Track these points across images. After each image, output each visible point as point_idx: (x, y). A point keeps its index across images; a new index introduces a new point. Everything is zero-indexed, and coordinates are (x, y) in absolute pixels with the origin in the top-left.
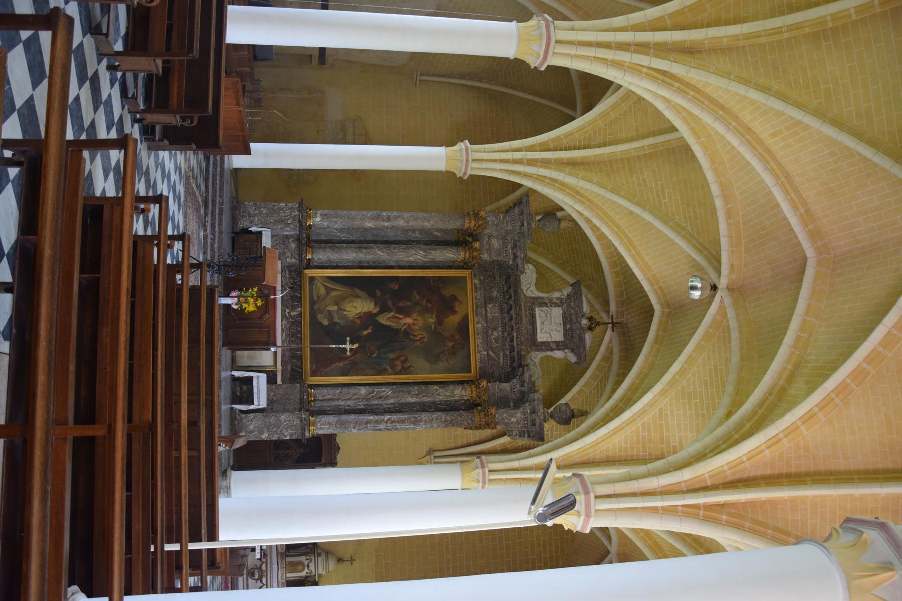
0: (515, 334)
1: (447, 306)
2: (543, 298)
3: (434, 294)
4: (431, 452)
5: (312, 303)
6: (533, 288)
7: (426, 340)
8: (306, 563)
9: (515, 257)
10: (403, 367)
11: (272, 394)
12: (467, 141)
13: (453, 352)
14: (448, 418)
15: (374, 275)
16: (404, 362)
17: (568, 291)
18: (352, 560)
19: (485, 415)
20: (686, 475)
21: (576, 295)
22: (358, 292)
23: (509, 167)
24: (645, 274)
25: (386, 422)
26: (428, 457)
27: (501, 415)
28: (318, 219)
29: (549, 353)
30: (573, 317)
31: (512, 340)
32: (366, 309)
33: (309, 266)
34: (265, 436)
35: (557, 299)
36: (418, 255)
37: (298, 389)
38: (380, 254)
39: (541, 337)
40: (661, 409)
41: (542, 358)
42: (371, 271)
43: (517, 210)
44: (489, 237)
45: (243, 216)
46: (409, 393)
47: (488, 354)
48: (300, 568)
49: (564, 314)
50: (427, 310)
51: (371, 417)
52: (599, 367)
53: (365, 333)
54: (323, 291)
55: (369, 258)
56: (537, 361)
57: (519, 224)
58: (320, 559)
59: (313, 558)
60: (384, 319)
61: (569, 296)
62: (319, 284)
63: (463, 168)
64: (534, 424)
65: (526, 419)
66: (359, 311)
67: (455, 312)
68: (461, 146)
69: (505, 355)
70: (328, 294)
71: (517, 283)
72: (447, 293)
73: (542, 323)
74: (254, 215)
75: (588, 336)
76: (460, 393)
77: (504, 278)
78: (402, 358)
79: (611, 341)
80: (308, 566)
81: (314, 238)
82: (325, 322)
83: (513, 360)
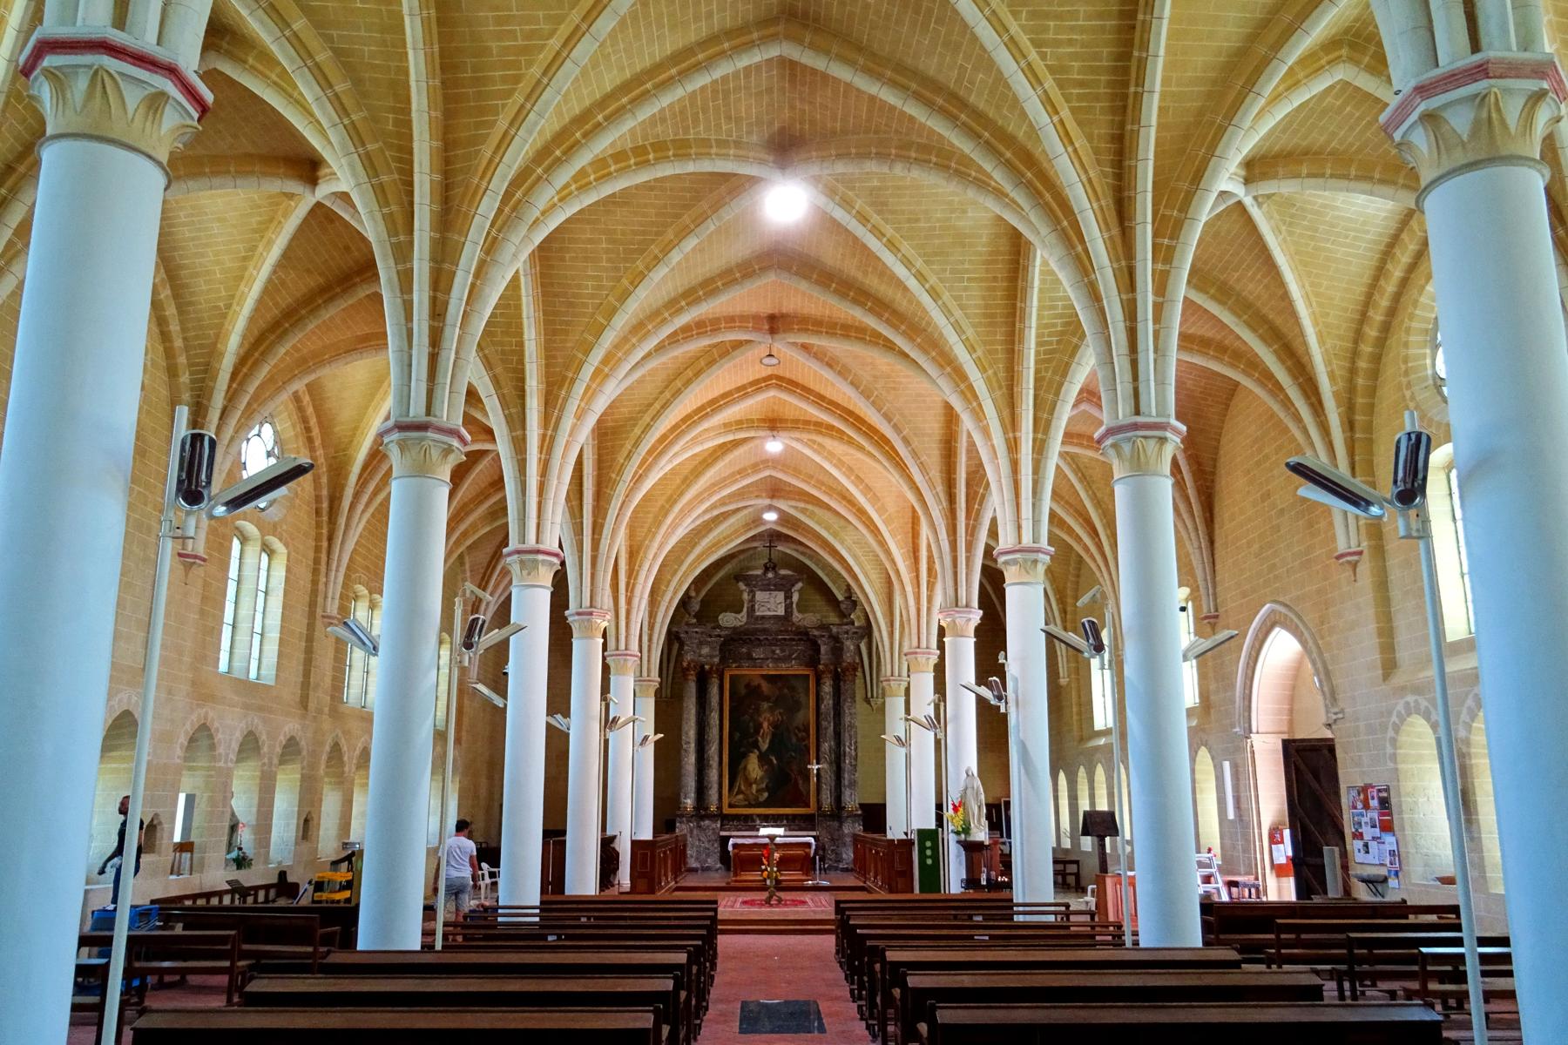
1: (754, 692)
3: (744, 702)
4: (867, 701)
5: (750, 806)
13: (793, 689)
17: (742, 586)
21: (748, 580)
27: (848, 657)
36: (715, 716)
38: (713, 750)
39: (781, 612)
50: (758, 711)
60: (765, 746)
72: (743, 691)
75: (783, 572)
76: (827, 688)
77: (734, 644)
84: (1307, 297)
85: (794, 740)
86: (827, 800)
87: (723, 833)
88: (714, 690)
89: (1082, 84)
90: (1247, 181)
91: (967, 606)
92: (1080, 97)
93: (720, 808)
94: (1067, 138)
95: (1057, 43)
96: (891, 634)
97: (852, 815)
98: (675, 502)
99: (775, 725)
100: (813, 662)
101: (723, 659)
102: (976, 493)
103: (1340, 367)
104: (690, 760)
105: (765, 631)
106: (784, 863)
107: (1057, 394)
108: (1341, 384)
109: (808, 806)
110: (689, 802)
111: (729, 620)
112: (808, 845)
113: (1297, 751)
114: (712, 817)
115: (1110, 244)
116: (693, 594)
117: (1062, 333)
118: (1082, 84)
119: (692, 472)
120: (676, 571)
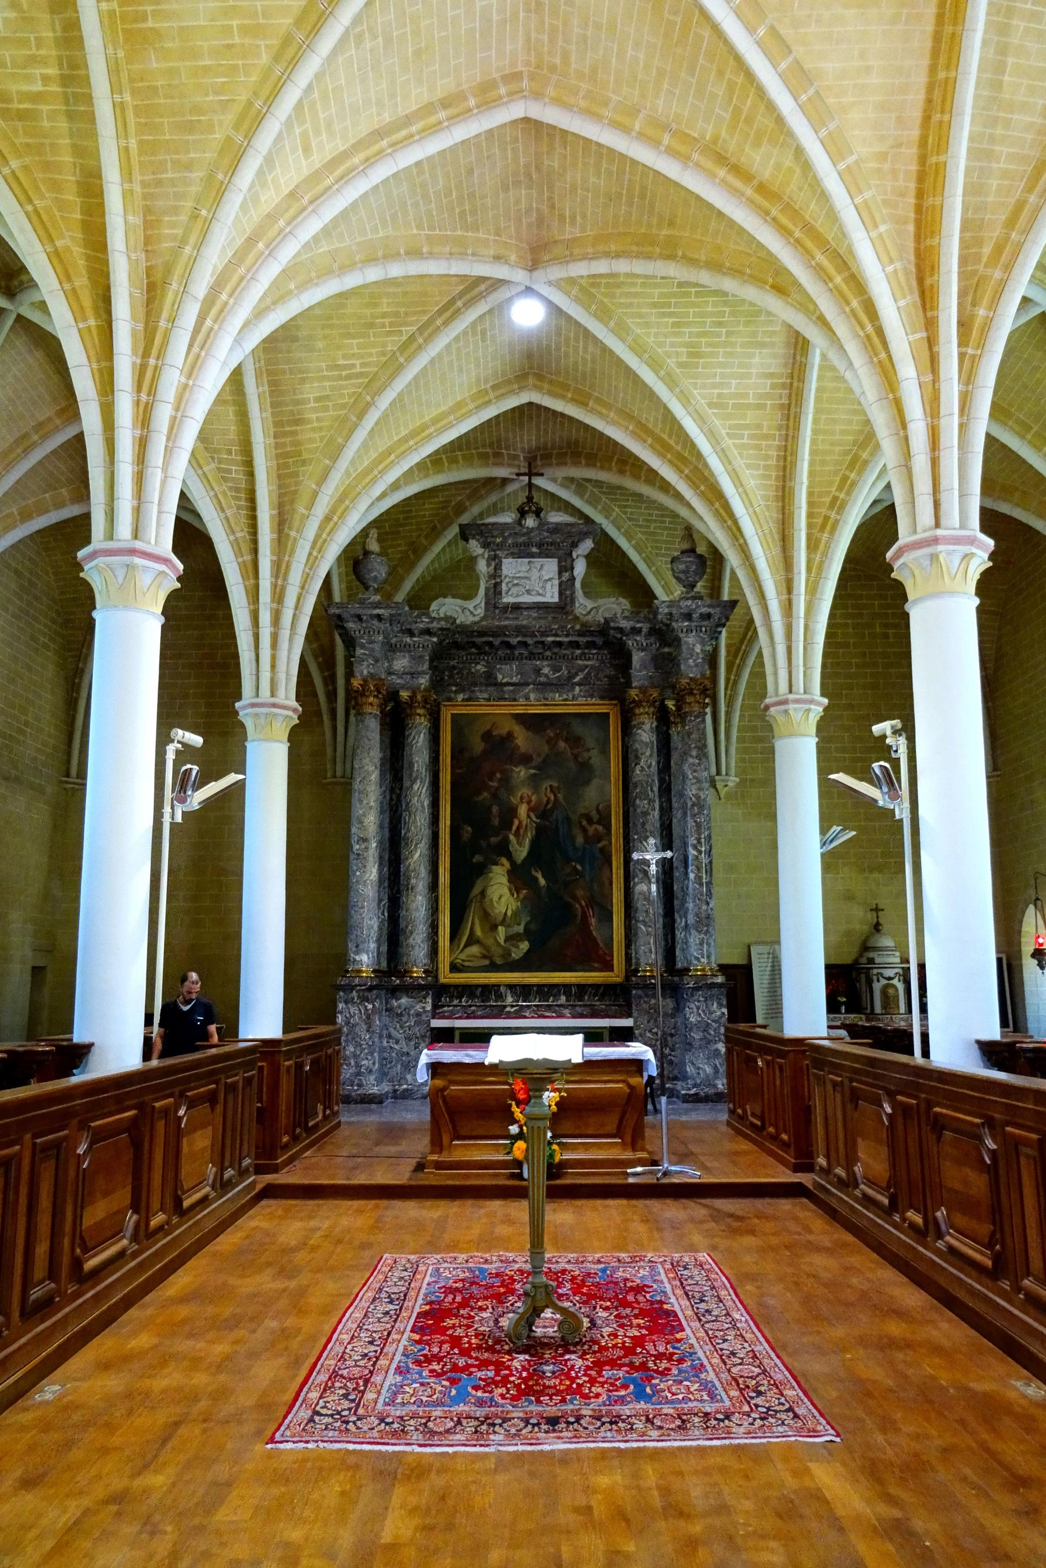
0: (550, 639)
1: (499, 746)
2: (487, 589)
5: (493, 967)
6: (470, 605)
7: (555, 784)
8: (884, 982)
9: (428, 632)
10: (599, 823)
11: (648, 1034)
12: (237, 705)
13: (576, 741)
14: (694, 753)
15: (448, 865)
16: (590, 821)
17: (475, 547)
18: (877, 910)
19: (691, 693)
20: (908, 372)
22: (476, 891)
23: (285, 633)
24: (470, 414)
25: (700, 852)
26: (719, 786)
27: (691, 667)
28: (364, 958)
29: (578, 584)
30: (521, 540)
31: (559, 644)
32: (504, 880)
33: (432, 972)
34: (721, 1047)
35: (488, 565)
36: (419, 794)
37: (640, 992)
38: (417, 857)
39: (551, 595)
40: (710, 405)
41: (587, 595)
42: (441, 871)
43: (351, 625)
44: (390, 674)
45: (360, 1085)
46: (645, 814)
47: (579, 684)
48: (891, 991)
50: (506, 781)
51: (692, 876)
52: (593, 502)
53: (542, 881)
54: (474, 950)
55: (423, 872)
56: (589, 604)
57: (375, 622)
58: (878, 960)
59: (875, 971)
60: (521, 851)
61: (485, 545)
62: (463, 956)
64: (708, 616)
65: (698, 629)
66: (506, 891)
67: (510, 735)
68: (242, 715)
69: (581, 657)
70: (478, 942)
71: (464, 630)
72: (478, 746)
73: (528, 592)
74: (358, 1066)
75: (556, 518)
76: (646, 734)
77: (457, 653)
78: (584, 823)
79: (554, 480)
81: (384, 965)
82: (525, 946)
83: (591, 645)
85: (580, 840)
86: (649, 955)
87: (436, 1023)
88: (419, 740)
93: (432, 972)
96: (788, 608)
97: (704, 986)
98: (259, 119)
99: (543, 813)
100: (617, 689)
101: (437, 684)
104: (368, 876)
105: (519, 630)
106: (573, 1114)
109: (608, 966)
110: (365, 961)
111: (447, 608)
112: (638, 1065)
114: (414, 989)
116: (374, 546)
120: (324, 477)
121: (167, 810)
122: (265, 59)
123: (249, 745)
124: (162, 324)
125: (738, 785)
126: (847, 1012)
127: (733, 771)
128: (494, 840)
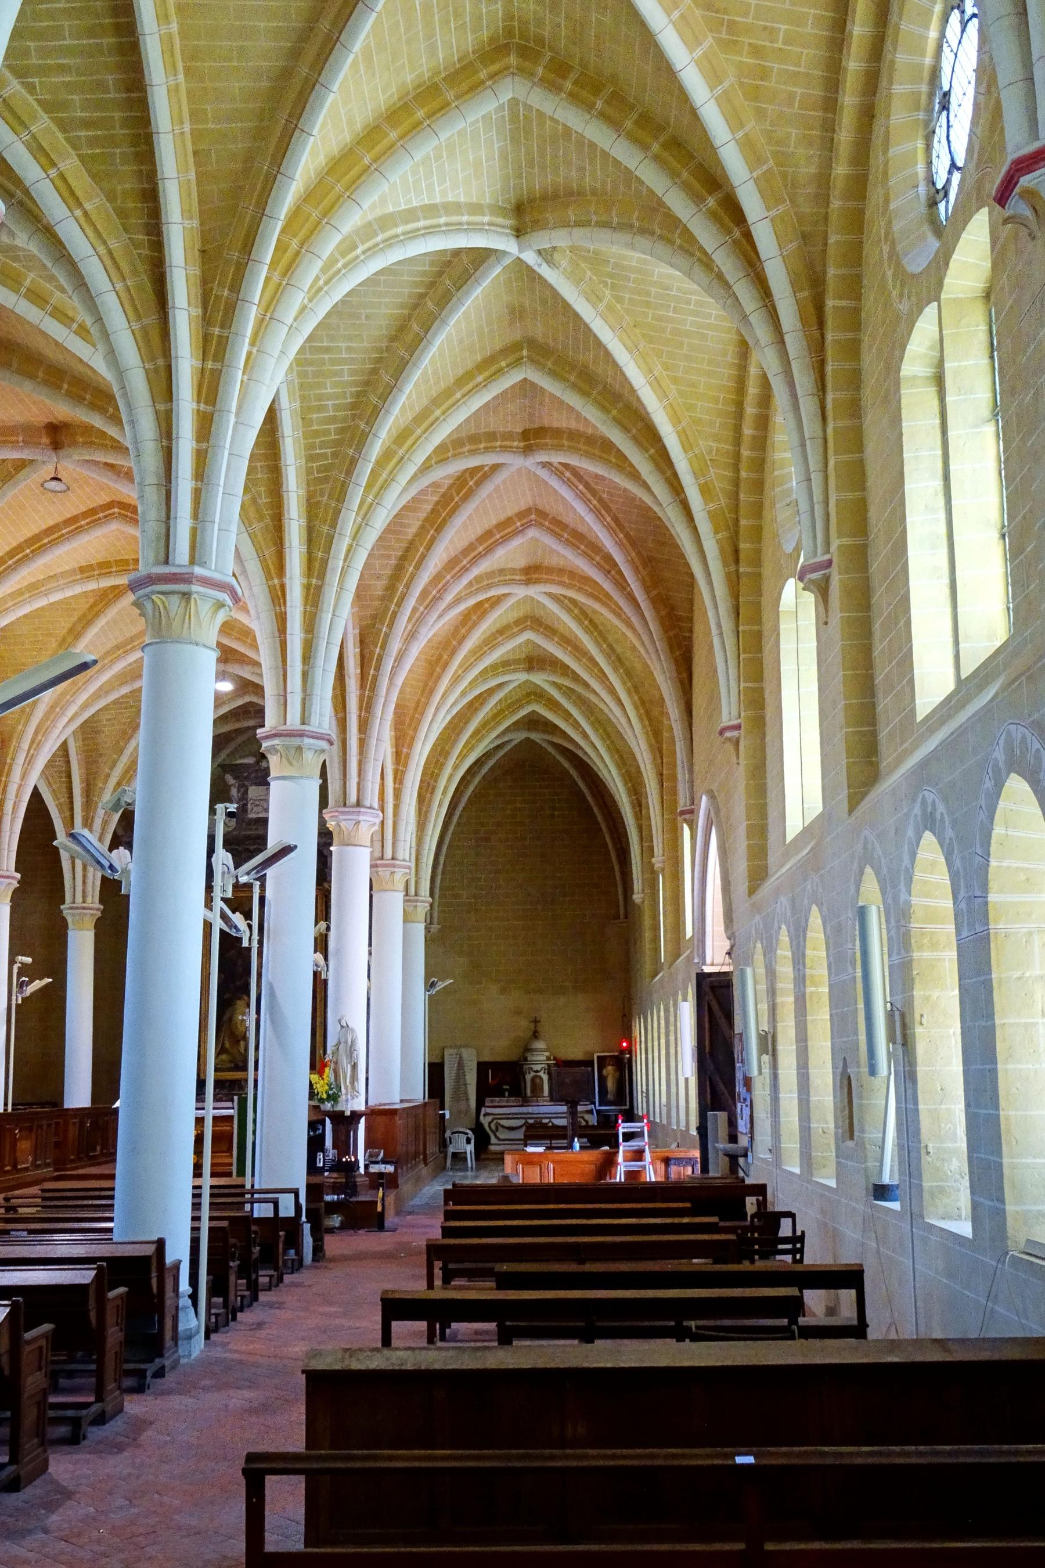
8: (533, 1074)
12: (62, 907)
48: (538, 1081)
49: (256, 784)
63: (92, 912)
68: (67, 913)
80: (537, 1071)
84: (656, 384)
89: (88, 124)
90: (519, 232)
91: (358, 804)
92: (92, 142)
94: (71, 197)
95: (43, 71)
102: (372, 653)
103: (719, 477)
107: (334, 525)
108: (723, 501)
113: (713, 988)
115: (144, 340)
117: (338, 443)
118: (88, 124)
119: (71, 630)
120: (114, 764)
121: (14, 998)
122: (54, 645)
123: (70, 933)
124: (9, 761)
125: (440, 930)
126: (509, 1096)
127: (436, 920)
128: (238, 983)
